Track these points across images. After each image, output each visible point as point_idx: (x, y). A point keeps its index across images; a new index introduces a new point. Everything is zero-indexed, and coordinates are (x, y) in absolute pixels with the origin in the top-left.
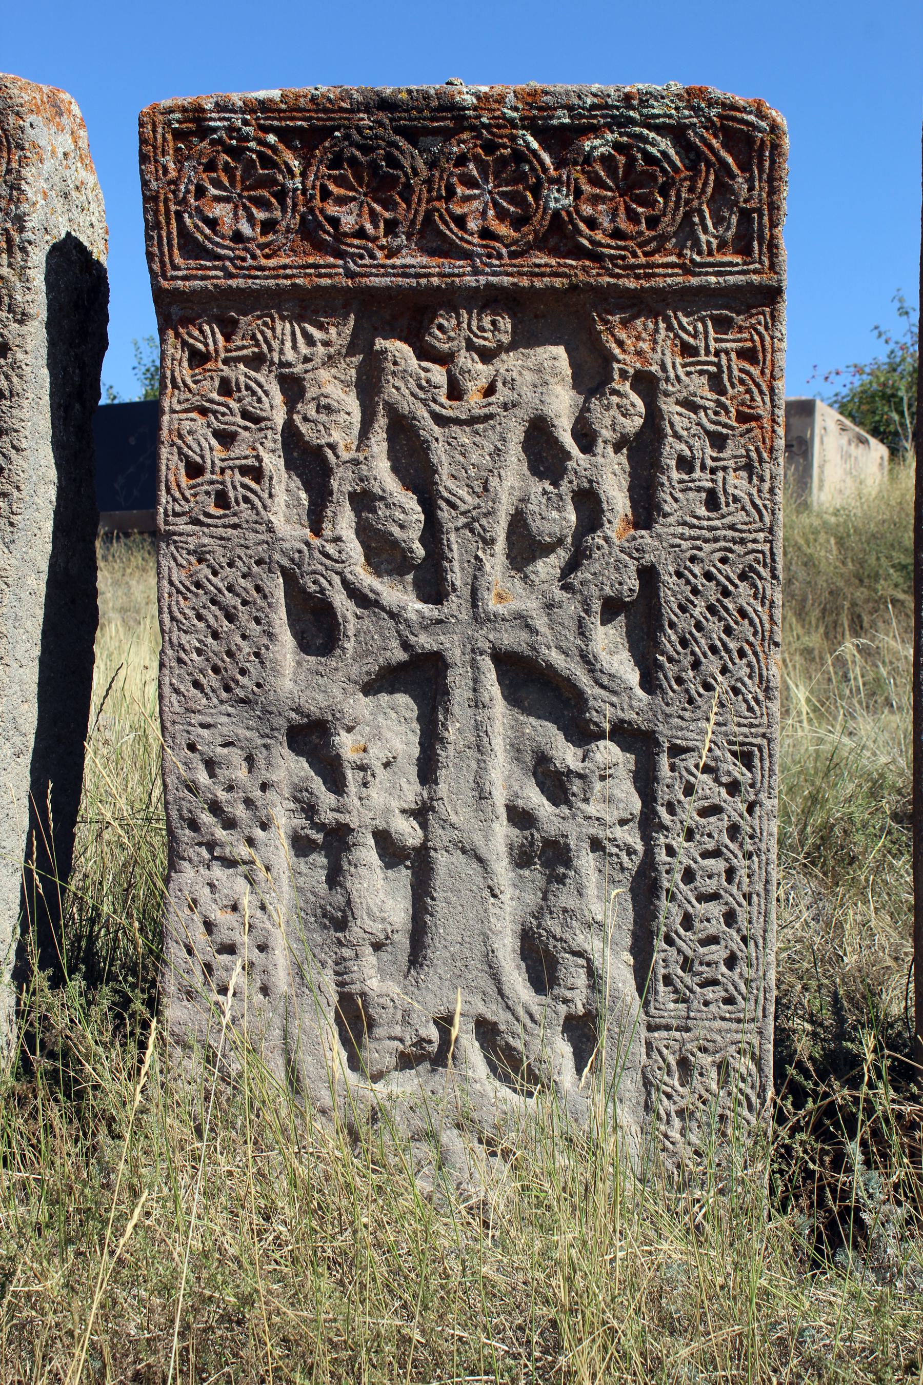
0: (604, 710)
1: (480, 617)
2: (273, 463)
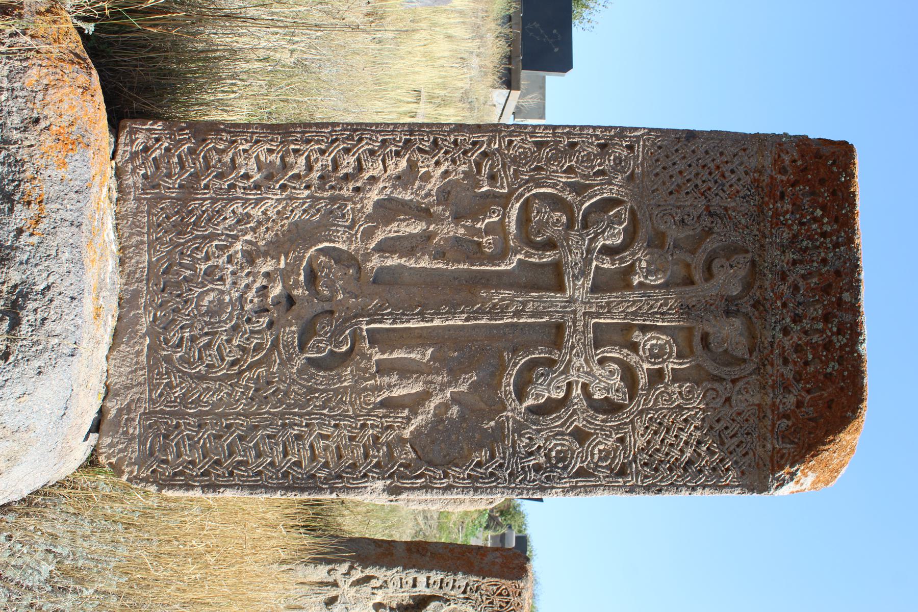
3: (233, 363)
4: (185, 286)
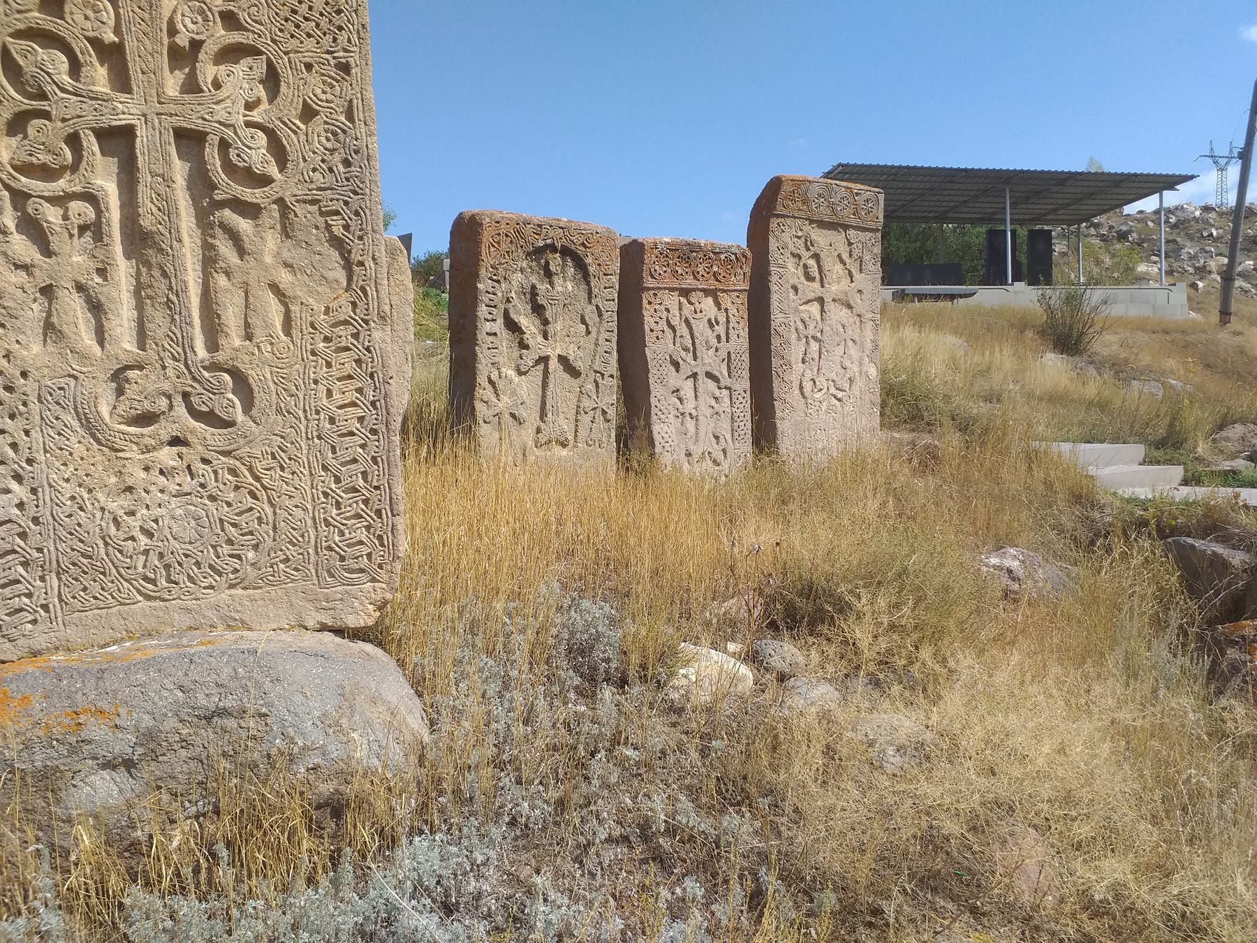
0: (723, 384)
1: (704, 364)
2: (666, 328)
3: (253, 495)
4: (167, 560)
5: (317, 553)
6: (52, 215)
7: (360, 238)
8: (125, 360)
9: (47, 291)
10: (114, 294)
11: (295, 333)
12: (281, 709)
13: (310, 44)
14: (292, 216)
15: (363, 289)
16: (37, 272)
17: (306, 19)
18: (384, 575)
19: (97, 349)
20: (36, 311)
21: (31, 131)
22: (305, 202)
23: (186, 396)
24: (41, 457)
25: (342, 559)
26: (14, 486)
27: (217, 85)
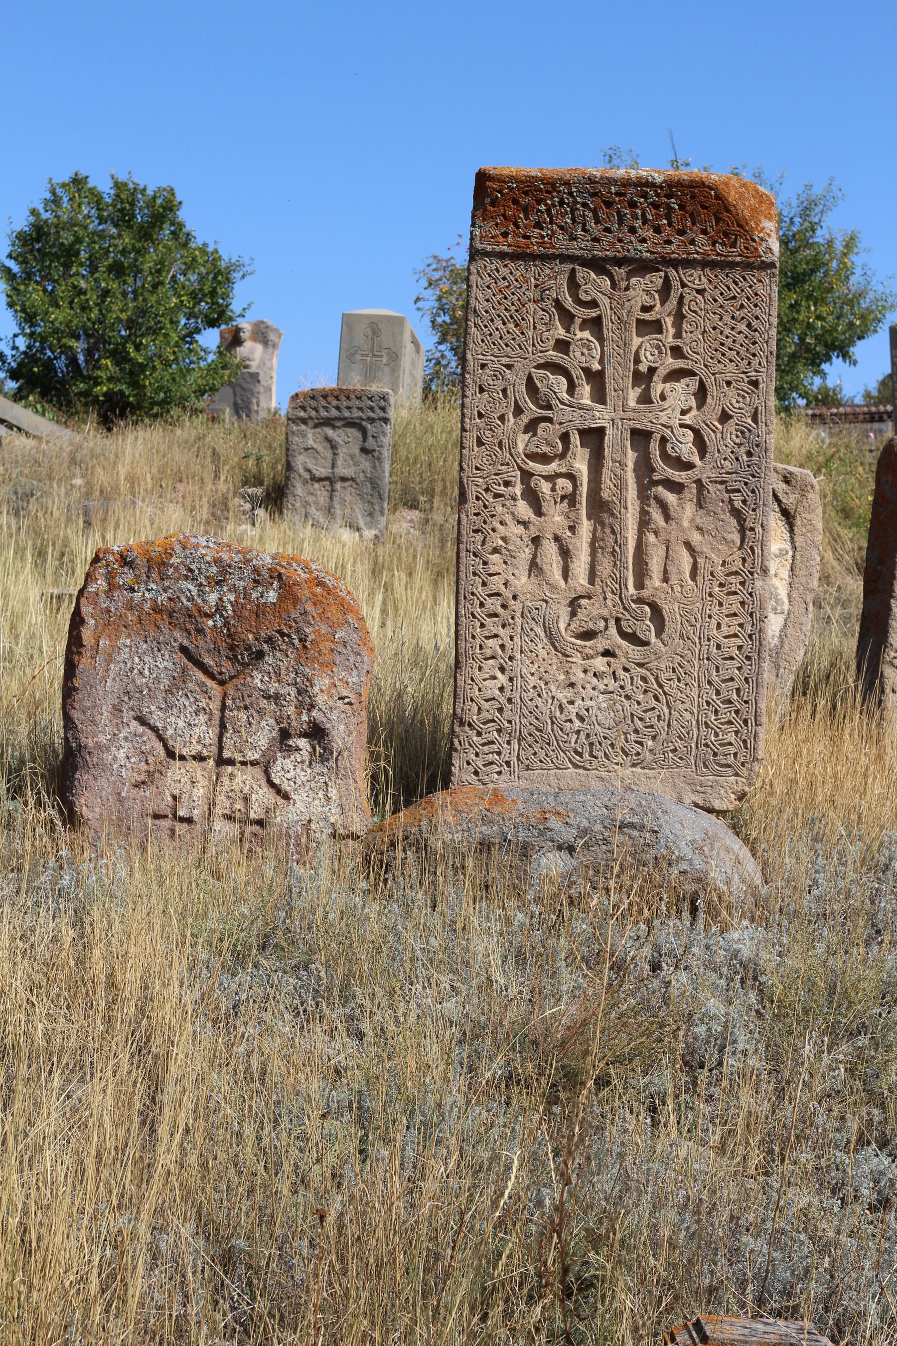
3: (656, 698)
5: (697, 748)
6: (545, 487)
7: (754, 510)
8: (581, 591)
9: (536, 541)
10: (579, 544)
11: (699, 579)
12: (666, 830)
13: (731, 367)
14: (705, 492)
15: (752, 548)
16: (531, 527)
17: (730, 349)
18: (744, 772)
19: (562, 583)
20: (526, 554)
21: (539, 431)
22: (716, 482)
23: (618, 620)
24: (518, 656)
25: (715, 754)
26: (499, 674)
27: (663, 397)
